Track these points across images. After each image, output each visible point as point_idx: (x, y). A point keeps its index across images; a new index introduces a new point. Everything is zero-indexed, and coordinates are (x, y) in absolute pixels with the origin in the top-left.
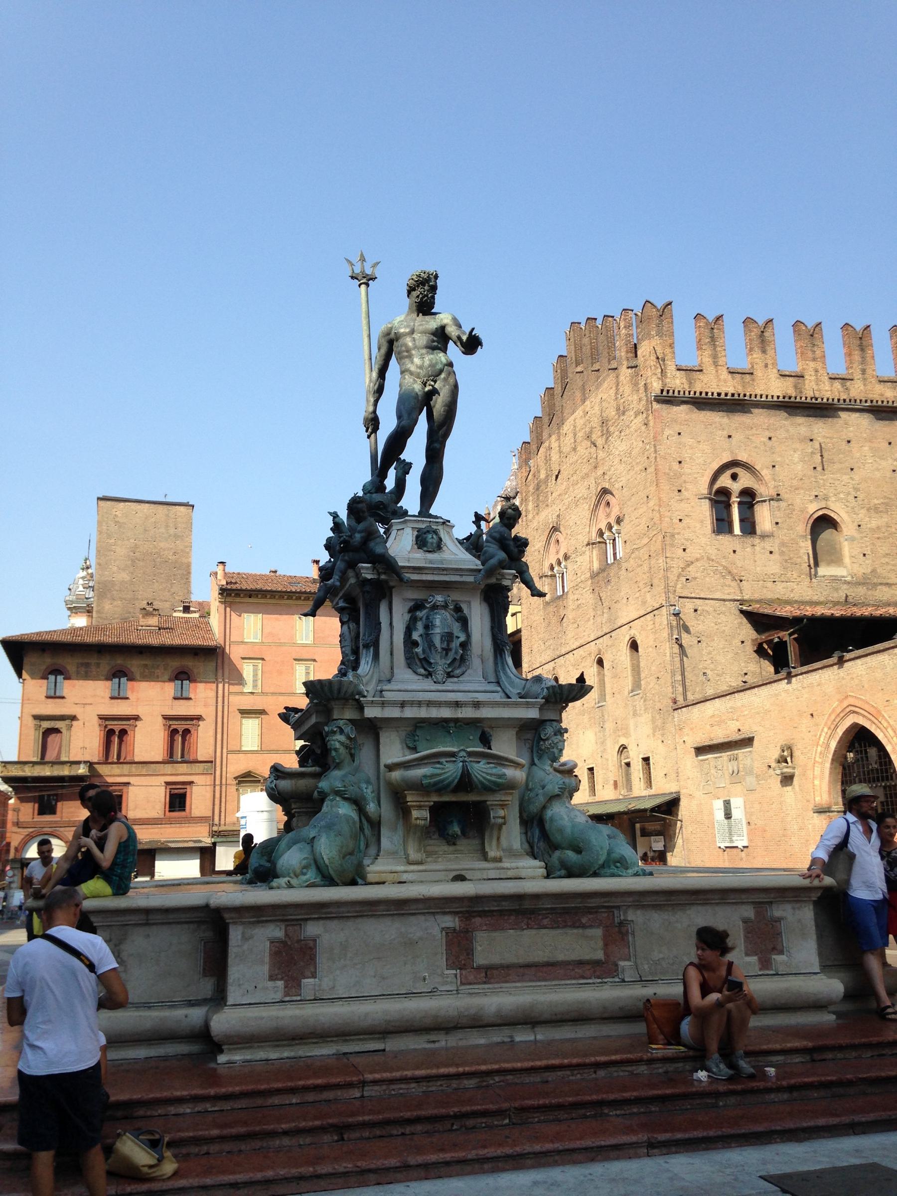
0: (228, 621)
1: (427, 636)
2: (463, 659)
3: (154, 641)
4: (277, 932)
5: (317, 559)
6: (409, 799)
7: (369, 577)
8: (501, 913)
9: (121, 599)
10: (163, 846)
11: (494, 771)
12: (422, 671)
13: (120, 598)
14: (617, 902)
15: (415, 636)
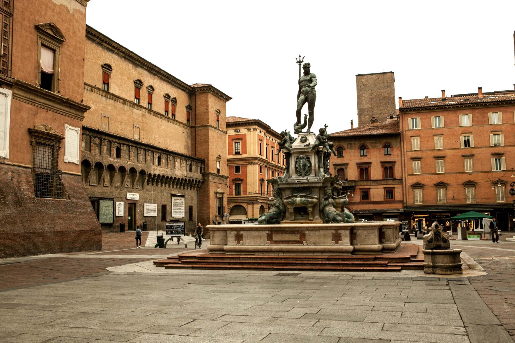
0: (404, 122)
1: (300, 166)
2: (310, 171)
3: (375, 133)
4: (236, 233)
5: (444, 90)
6: (288, 206)
7: (285, 152)
8: (279, 231)
9: (368, 115)
10: (385, 212)
11: (305, 200)
12: (299, 174)
13: (368, 115)
14: (302, 229)
15: (297, 166)
